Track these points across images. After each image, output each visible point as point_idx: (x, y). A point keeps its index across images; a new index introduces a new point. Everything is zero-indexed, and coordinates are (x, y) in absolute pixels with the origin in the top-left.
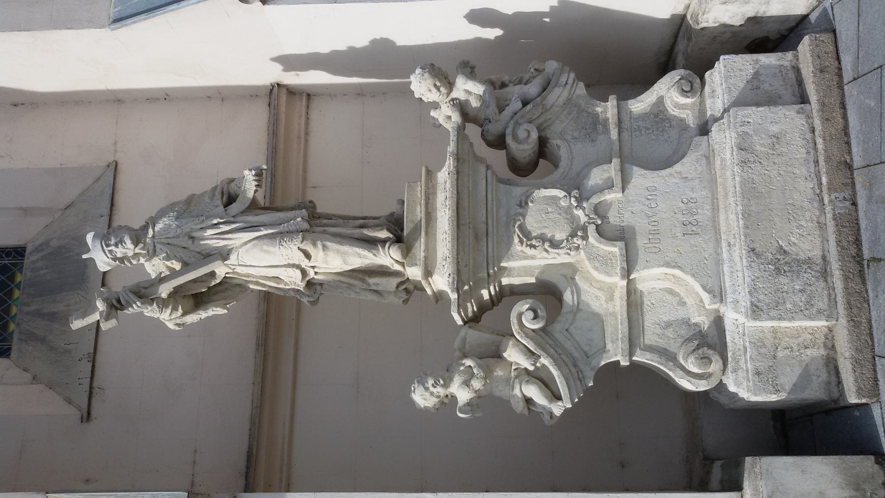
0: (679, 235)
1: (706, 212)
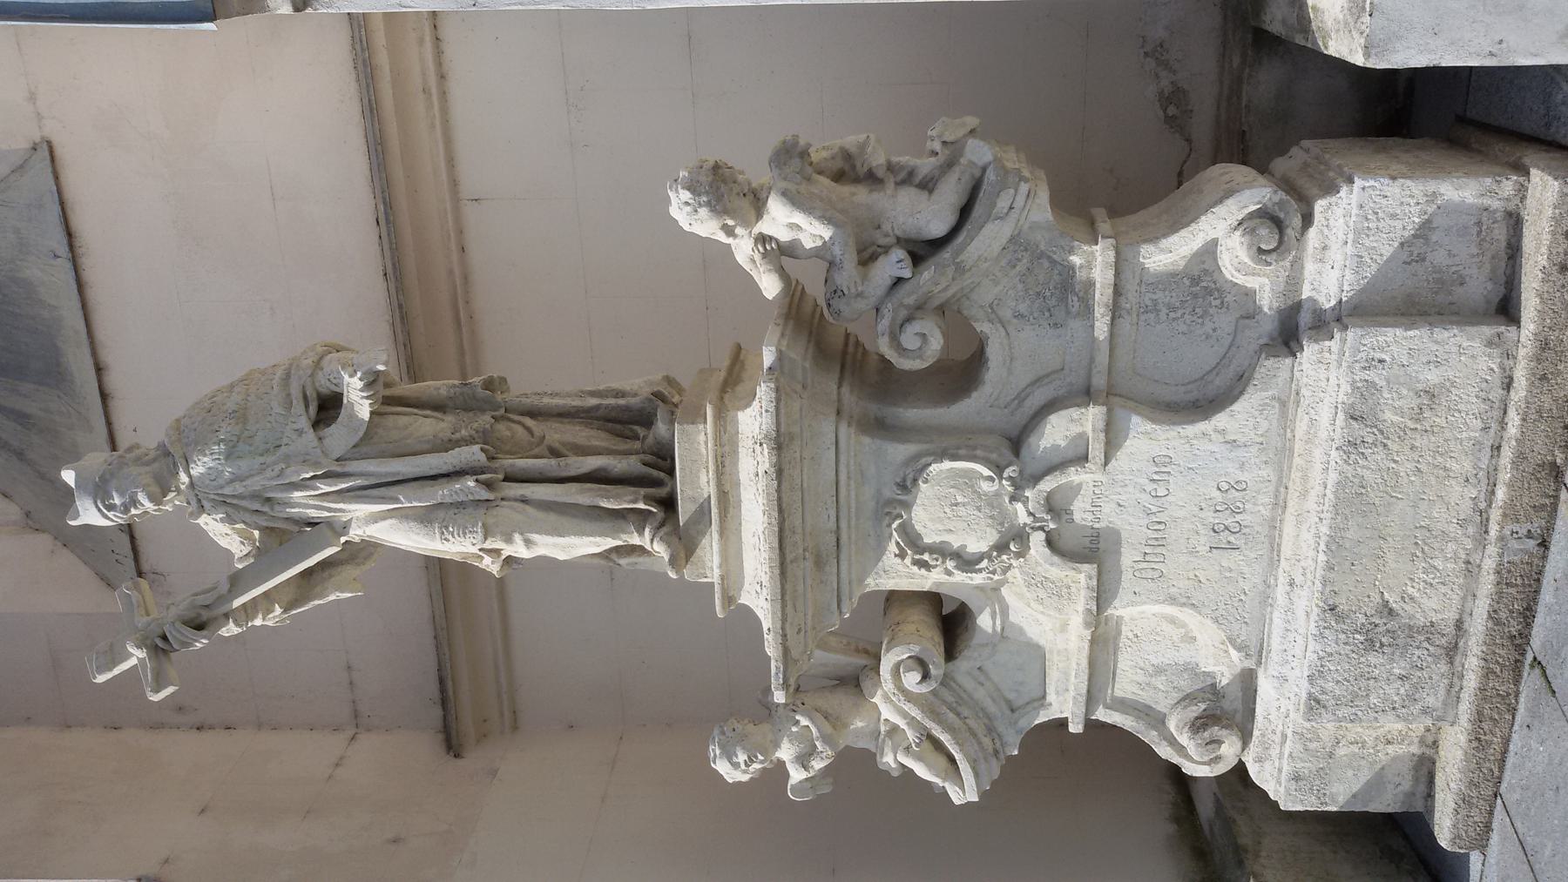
0: (1203, 549)
1: (1256, 513)
